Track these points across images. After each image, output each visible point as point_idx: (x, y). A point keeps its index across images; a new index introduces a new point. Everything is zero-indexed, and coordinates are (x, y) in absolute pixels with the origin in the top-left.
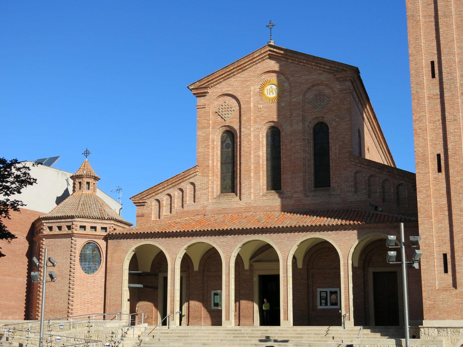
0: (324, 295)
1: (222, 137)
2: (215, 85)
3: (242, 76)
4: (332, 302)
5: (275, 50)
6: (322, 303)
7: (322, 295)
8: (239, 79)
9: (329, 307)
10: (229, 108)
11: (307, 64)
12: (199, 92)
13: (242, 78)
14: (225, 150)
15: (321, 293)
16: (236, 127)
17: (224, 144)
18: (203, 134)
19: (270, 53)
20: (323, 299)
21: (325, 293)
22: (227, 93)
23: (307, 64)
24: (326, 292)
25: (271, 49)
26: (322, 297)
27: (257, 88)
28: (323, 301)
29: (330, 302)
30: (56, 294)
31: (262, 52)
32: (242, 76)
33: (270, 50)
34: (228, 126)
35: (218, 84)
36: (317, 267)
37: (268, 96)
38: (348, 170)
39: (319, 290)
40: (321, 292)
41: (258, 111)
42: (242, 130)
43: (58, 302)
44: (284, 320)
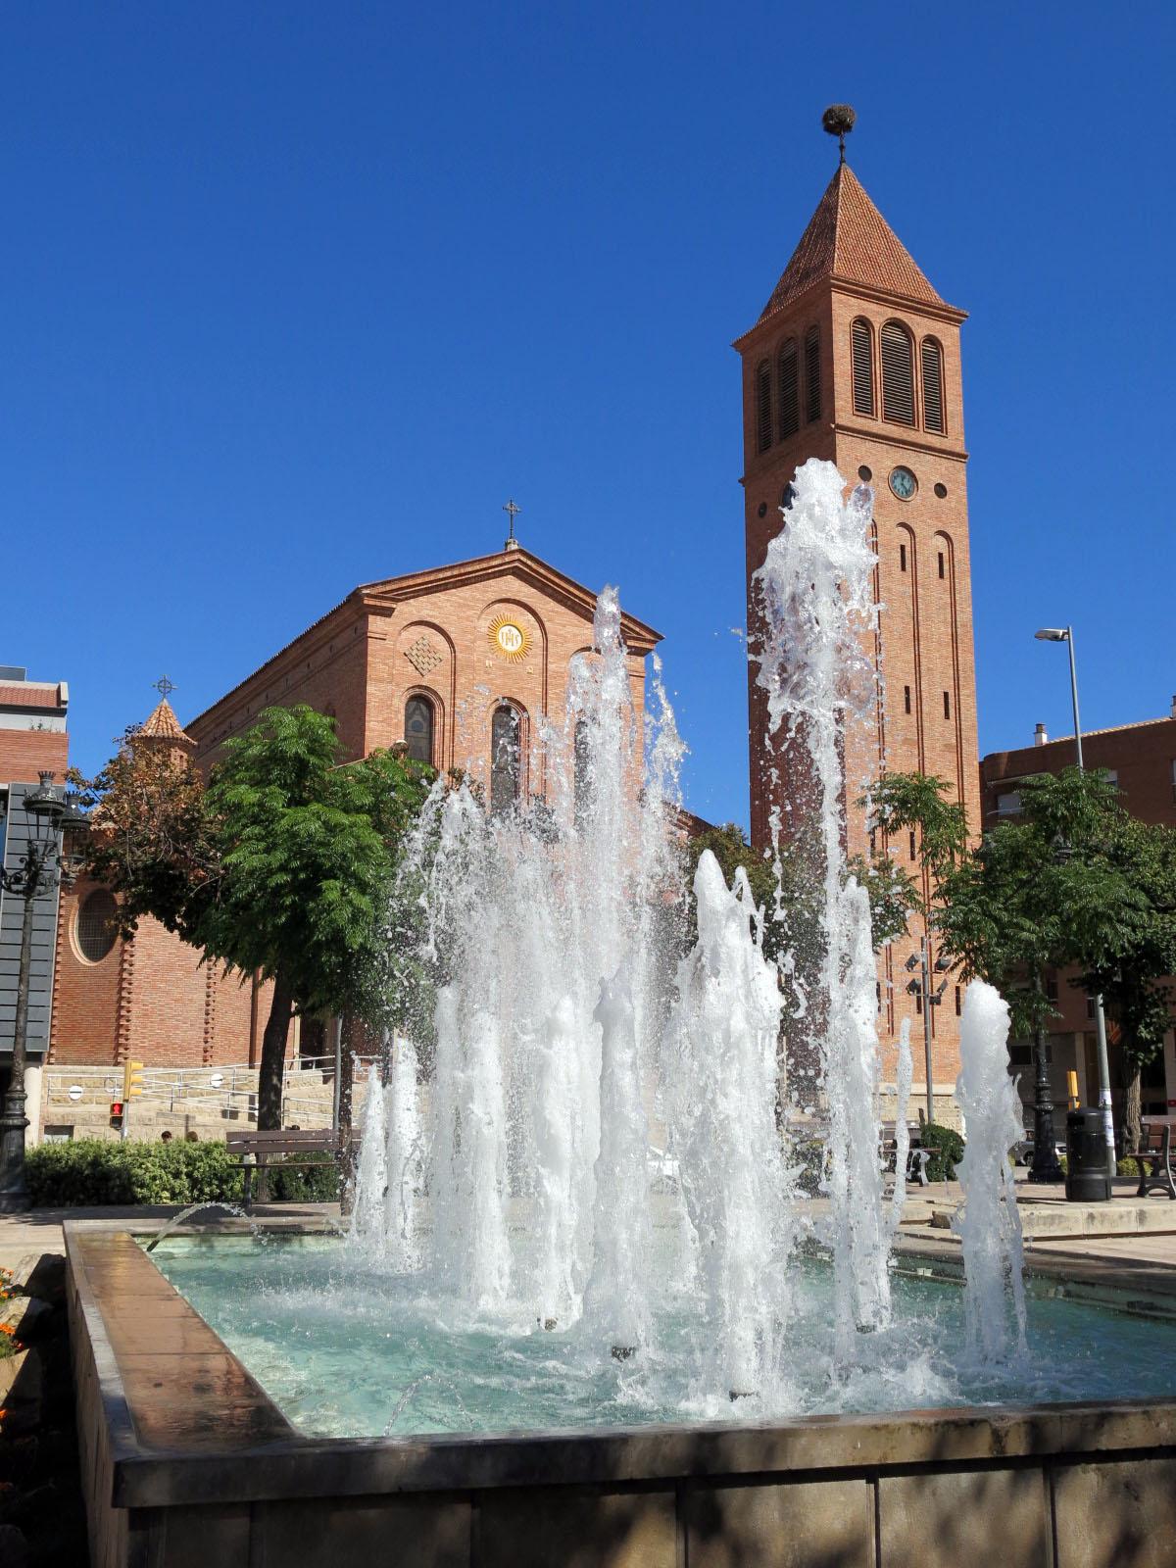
1: (407, 705)
2: (407, 599)
3: (461, 594)
5: (529, 562)
8: (454, 598)
10: (431, 650)
12: (378, 604)
13: (461, 598)
14: (411, 733)
16: (444, 692)
17: (410, 724)
18: (378, 693)
19: (517, 564)
22: (428, 619)
25: (522, 558)
27: (483, 625)
30: (171, 1008)
31: (507, 560)
32: (461, 594)
33: (519, 560)
34: (427, 688)
35: (413, 597)
37: (504, 646)
41: (486, 672)
42: (457, 701)
43: (177, 1027)
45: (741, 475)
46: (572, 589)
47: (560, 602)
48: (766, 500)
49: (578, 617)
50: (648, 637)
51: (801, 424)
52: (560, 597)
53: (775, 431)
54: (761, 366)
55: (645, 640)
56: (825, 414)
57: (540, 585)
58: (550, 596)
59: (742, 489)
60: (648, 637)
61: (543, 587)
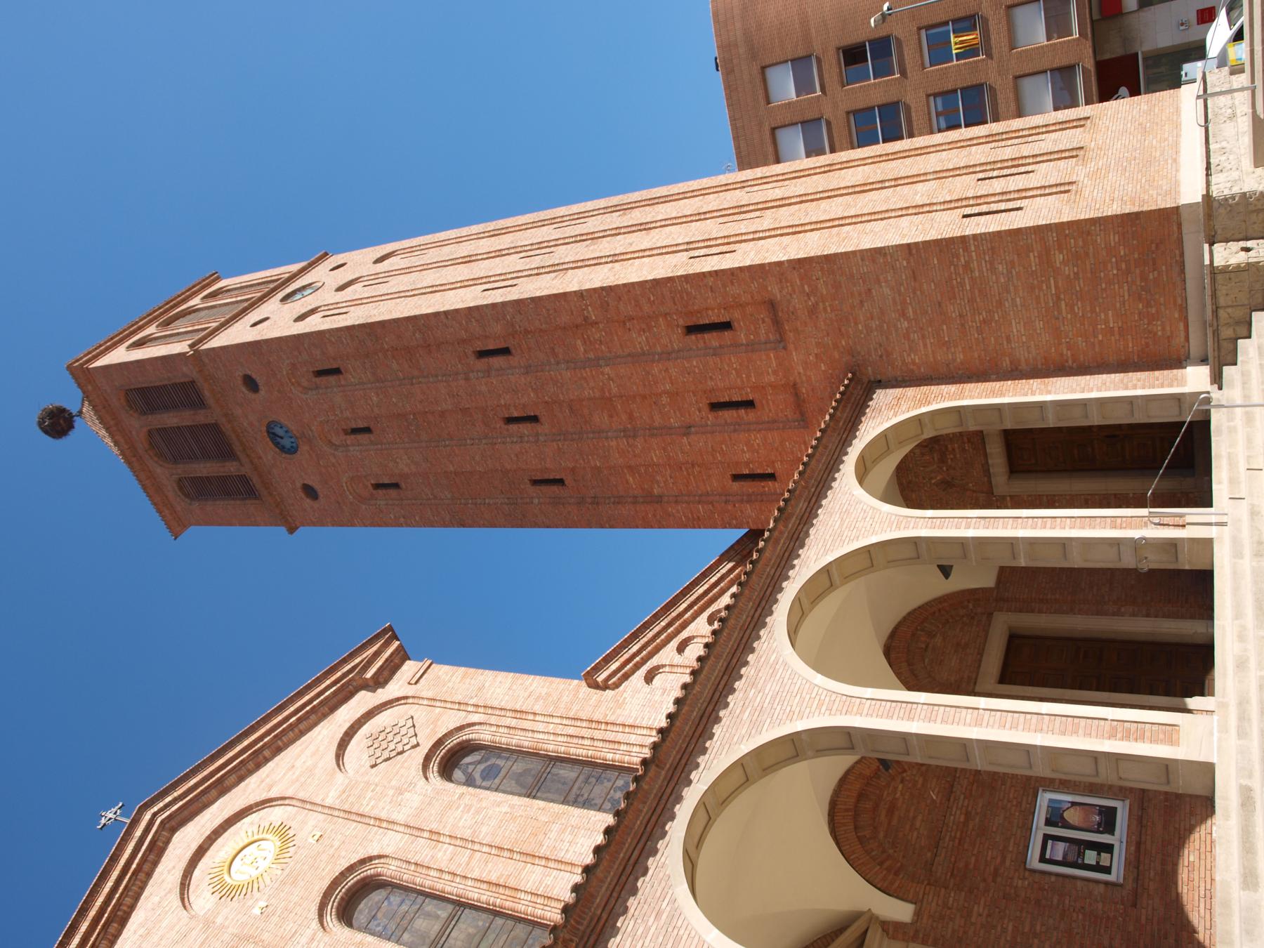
0: (1059, 851)
4: (1099, 827)
6: (1098, 863)
7: (1059, 857)
9: (1118, 838)
11: (280, 739)
15: (1047, 856)
20: (1081, 854)
21: (1050, 842)
23: (280, 739)
24: (1047, 838)
26: (1071, 858)
28: (1090, 857)
29: (1098, 832)
31: (138, 833)
33: (155, 815)
36: (929, 854)
38: (625, 698)
39: (1033, 861)
40: (1043, 859)
44: (1172, 741)
45: (282, 530)
46: (246, 743)
47: (258, 766)
48: (299, 485)
49: (298, 743)
50: (375, 648)
51: (211, 420)
52: (251, 765)
53: (231, 468)
54: (187, 495)
55: (377, 654)
56: (189, 372)
57: (214, 793)
58: (241, 779)
59: (302, 531)
60: (375, 648)
61: (221, 788)
